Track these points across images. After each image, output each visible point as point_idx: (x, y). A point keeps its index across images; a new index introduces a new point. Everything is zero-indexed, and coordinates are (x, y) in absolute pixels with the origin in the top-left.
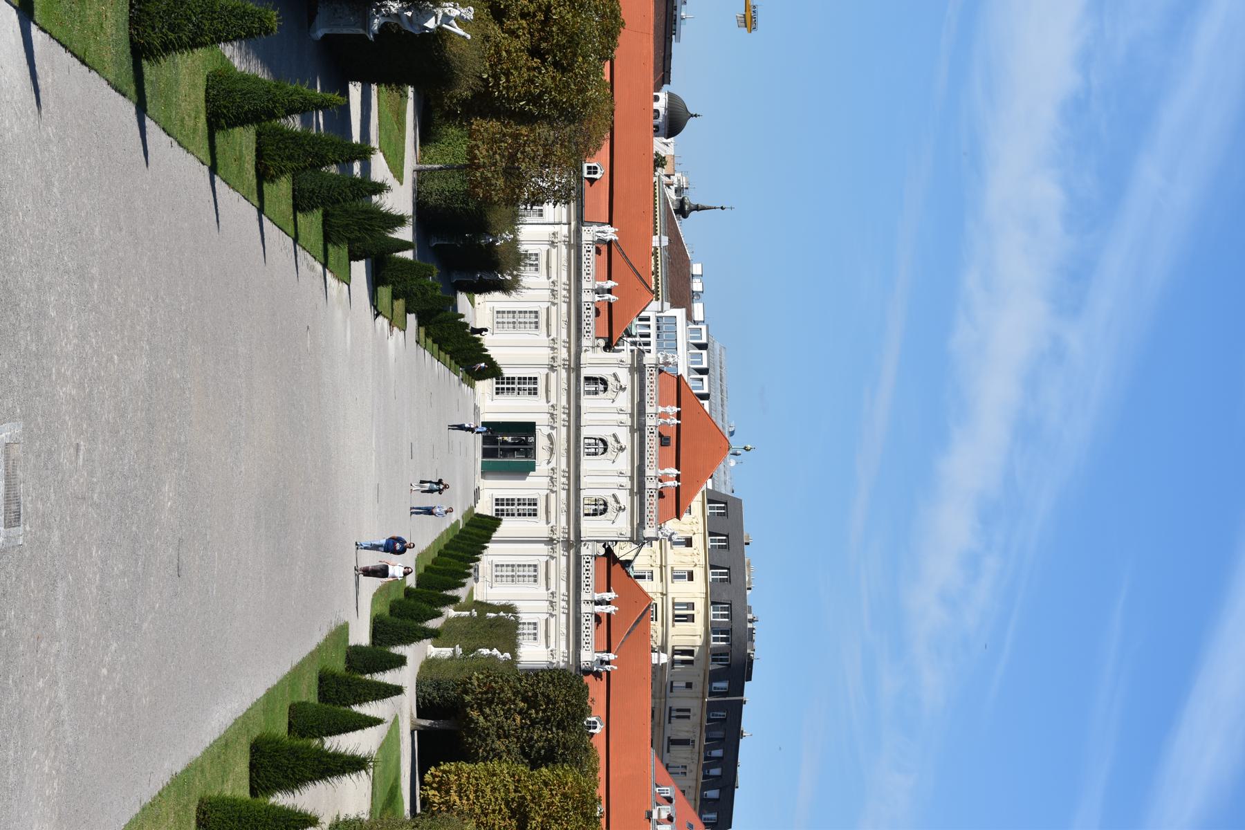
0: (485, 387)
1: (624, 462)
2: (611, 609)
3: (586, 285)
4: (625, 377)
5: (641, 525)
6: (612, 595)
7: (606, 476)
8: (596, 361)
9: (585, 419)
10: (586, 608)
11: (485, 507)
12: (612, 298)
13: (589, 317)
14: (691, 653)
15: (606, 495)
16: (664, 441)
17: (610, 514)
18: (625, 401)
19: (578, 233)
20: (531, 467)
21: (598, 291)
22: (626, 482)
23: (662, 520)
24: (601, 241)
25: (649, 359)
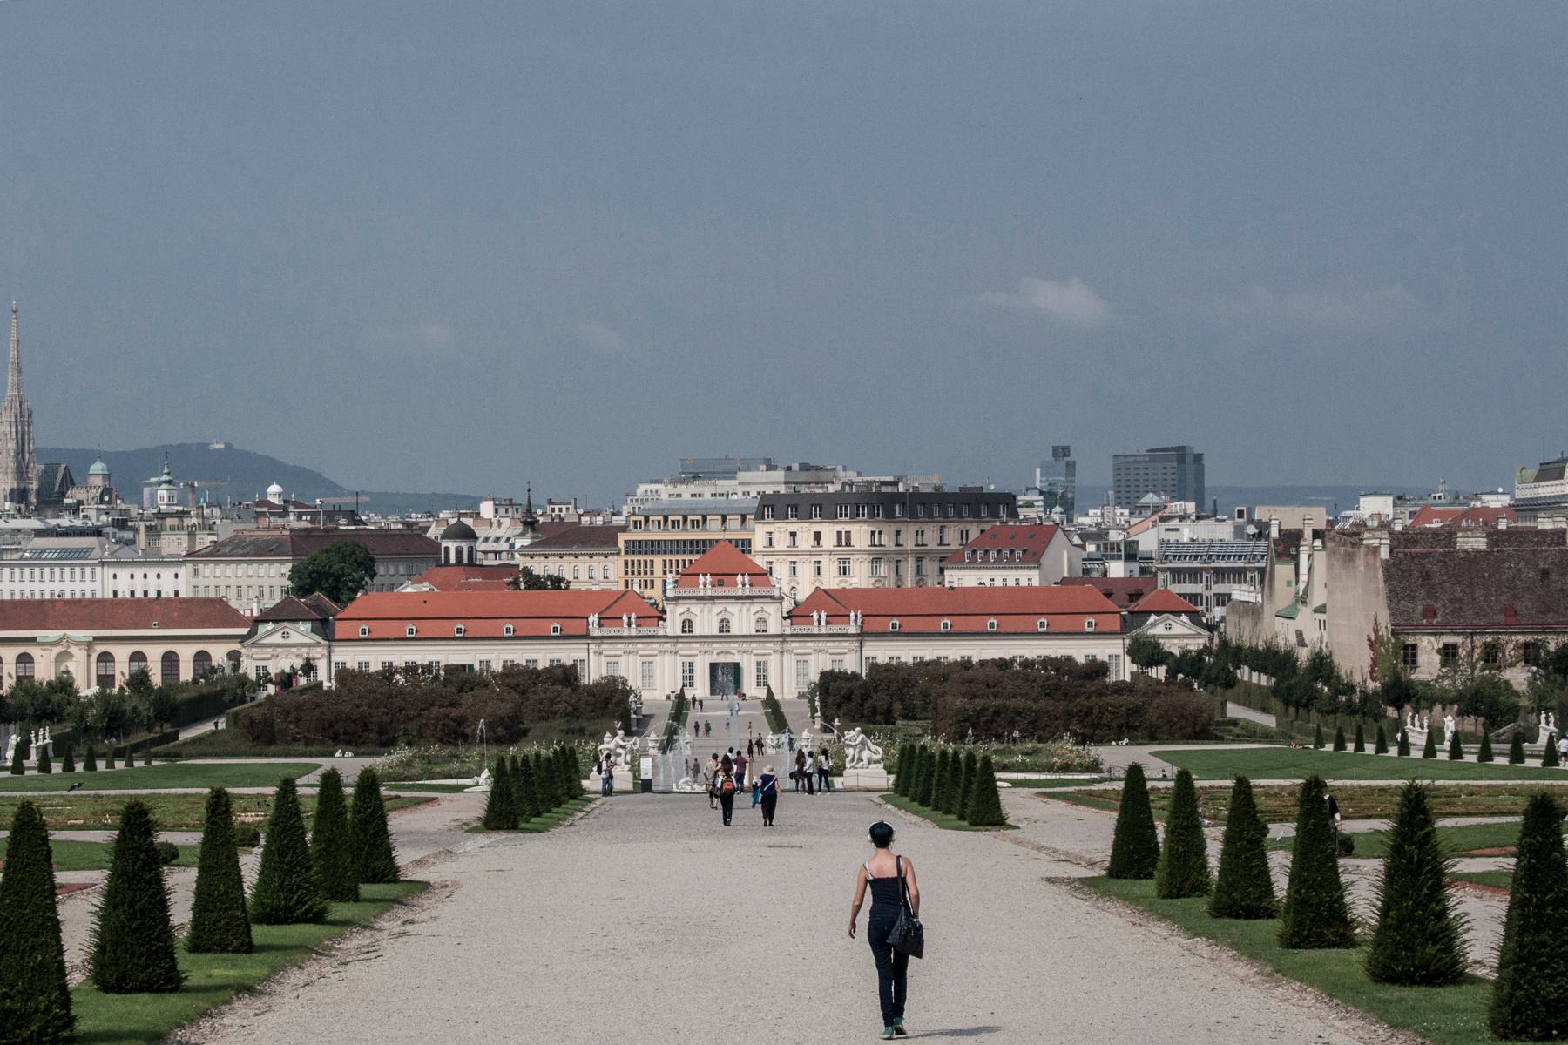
0: (688, 695)
1: (733, 608)
2: (823, 615)
3: (626, 633)
4: (681, 609)
5: (772, 597)
6: (815, 615)
7: (743, 619)
8: (672, 625)
9: (706, 633)
10: (823, 631)
11: (762, 693)
12: (633, 616)
13: (645, 631)
14: (873, 533)
15: (753, 620)
16: (721, 584)
17: (765, 616)
18: (696, 609)
19: (594, 638)
20: (737, 666)
21: (629, 625)
22: (745, 608)
23: (768, 584)
24: (600, 625)
25: (670, 594)
